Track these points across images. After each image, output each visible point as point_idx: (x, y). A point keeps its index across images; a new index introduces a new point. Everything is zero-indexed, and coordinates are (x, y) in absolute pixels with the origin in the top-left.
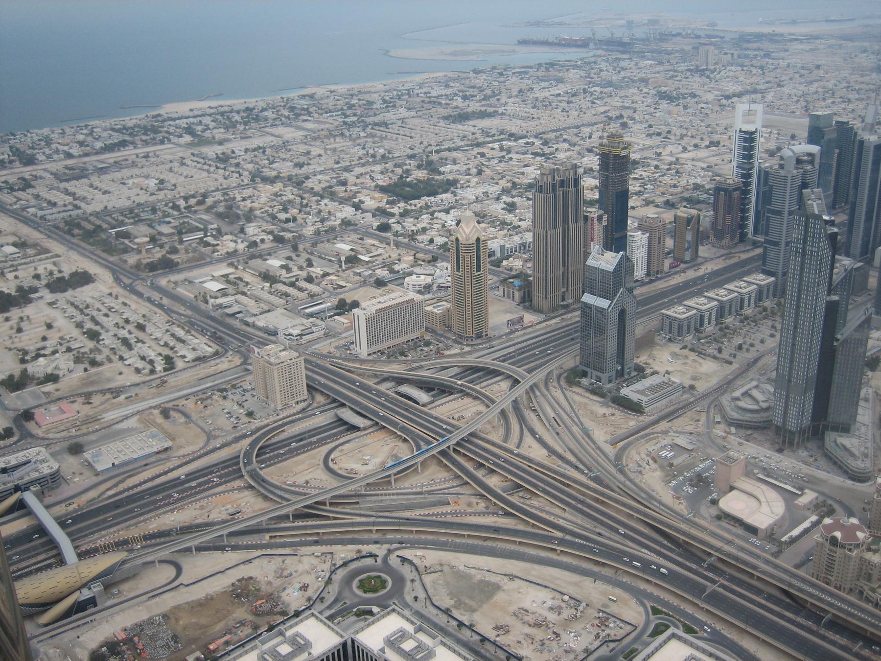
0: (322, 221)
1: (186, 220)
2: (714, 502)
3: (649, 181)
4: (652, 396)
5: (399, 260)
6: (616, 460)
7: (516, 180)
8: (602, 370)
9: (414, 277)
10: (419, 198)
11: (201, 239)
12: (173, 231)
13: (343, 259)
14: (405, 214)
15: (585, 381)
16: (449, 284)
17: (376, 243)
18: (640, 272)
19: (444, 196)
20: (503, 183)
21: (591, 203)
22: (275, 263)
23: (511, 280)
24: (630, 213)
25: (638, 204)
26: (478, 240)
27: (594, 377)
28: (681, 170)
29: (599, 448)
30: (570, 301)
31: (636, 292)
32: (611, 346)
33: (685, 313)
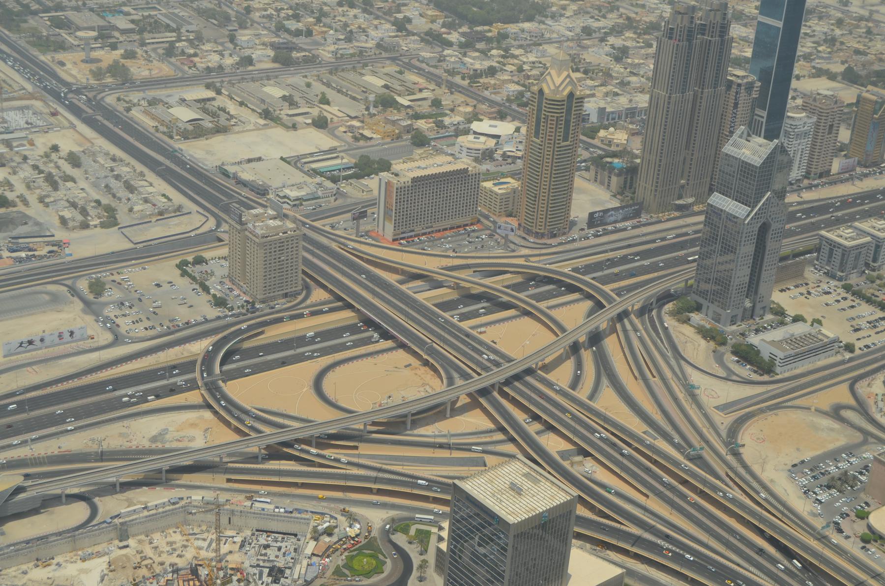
0: (349, 40)
1: (152, 13)
2: (863, 516)
3: (825, 41)
4: (792, 352)
5: (452, 110)
6: (728, 436)
7: (633, 15)
8: (724, 308)
9: (471, 137)
10: (490, 24)
11: (172, 44)
12: (132, 26)
13: (372, 97)
14: (466, 46)
15: (696, 317)
16: (520, 154)
17: (421, 81)
18: (795, 173)
19: (527, 25)
20: (613, 19)
21: (739, 62)
22: (274, 92)
23: (609, 160)
24: (794, 84)
25: (805, 73)
26: (571, 95)
27: (710, 313)
28: (875, 31)
29: (706, 416)
30: (691, 200)
31: (786, 201)
32: (742, 274)
33: (854, 239)
